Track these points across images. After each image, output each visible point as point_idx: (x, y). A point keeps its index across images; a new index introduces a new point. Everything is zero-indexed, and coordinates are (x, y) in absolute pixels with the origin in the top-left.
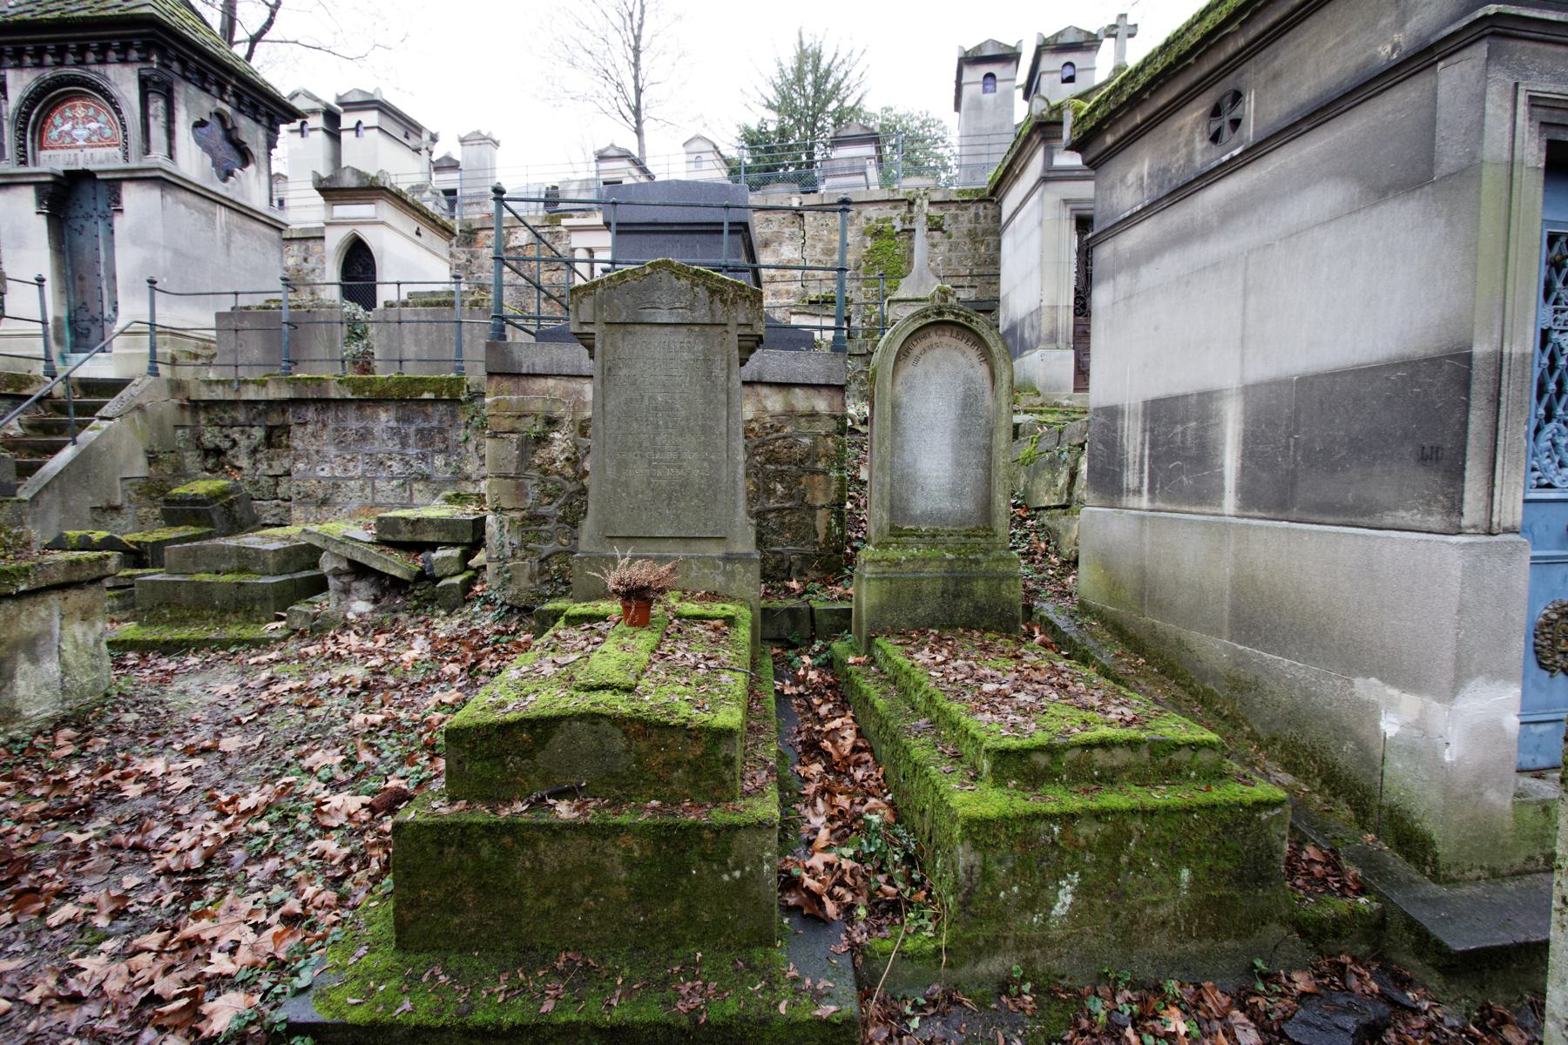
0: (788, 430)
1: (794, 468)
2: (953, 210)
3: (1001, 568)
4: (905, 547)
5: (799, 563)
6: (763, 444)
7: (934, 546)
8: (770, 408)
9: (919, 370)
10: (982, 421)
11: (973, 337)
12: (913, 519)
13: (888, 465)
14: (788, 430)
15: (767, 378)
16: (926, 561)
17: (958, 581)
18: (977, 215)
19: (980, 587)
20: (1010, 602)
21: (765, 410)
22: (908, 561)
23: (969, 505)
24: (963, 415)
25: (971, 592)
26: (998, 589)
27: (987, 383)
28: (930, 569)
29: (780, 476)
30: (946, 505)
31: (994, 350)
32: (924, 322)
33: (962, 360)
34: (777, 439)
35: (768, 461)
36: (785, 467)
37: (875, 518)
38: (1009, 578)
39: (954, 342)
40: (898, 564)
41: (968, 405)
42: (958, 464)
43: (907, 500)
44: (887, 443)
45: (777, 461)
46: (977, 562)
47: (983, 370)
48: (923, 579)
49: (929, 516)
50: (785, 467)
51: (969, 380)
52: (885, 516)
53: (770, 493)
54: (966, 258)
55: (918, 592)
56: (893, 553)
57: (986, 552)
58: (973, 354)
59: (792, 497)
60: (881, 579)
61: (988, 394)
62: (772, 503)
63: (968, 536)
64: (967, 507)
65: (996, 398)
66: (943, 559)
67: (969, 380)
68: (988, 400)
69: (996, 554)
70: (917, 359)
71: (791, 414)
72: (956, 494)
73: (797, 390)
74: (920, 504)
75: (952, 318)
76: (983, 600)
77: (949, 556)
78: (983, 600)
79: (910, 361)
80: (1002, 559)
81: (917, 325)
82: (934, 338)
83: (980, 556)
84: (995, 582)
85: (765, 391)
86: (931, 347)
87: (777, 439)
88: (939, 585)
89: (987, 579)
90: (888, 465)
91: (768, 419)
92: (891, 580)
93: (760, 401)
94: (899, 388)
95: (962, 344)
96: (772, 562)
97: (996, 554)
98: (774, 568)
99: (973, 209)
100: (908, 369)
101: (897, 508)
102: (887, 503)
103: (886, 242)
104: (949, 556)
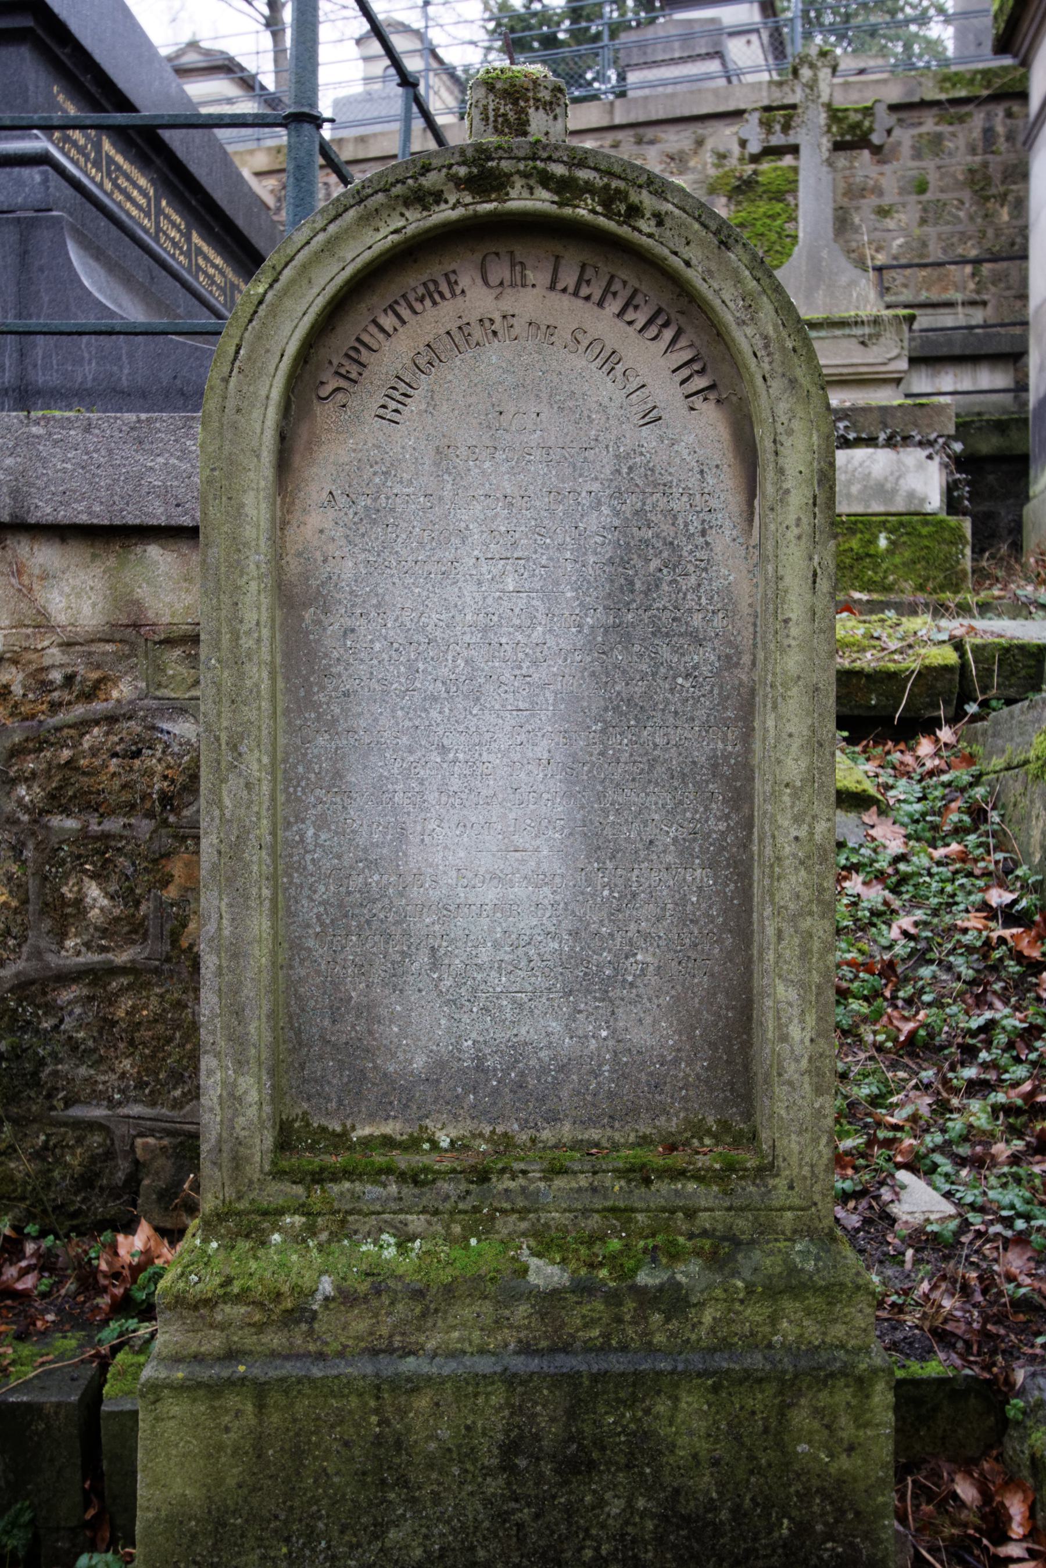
0: (123, 691)
1: (145, 826)
2: (929, 124)
3: (794, 1325)
4: (342, 1230)
5: (164, 1165)
6: (39, 743)
7: (480, 1223)
8: (61, 618)
9: (408, 438)
10: (706, 657)
11: (654, 296)
12: (398, 1094)
13: (258, 861)
14: (123, 691)
15: (44, 511)
16: (429, 1299)
17: (580, 1394)
18: (989, 133)
19: (687, 1422)
20: (837, 1493)
21: (43, 623)
22: (346, 1298)
23: (649, 1028)
24: (619, 632)
25: (643, 1447)
26: (777, 1434)
27: (724, 487)
28: (459, 1338)
29: (99, 854)
30: (547, 1030)
31: (744, 338)
32: (416, 221)
33: (604, 390)
34: (84, 725)
35: (56, 802)
36: (113, 825)
37: (233, 1097)
38: (825, 1377)
39: (567, 312)
40: (299, 1314)
41: (639, 590)
42: (596, 845)
43: (368, 1011)
44: (255, 762)
45: (90, 803)
46: (674, 1301)
47: (704, 431)
48: (414, 1385)
49: (465, 1081)
50: (113, 825)
51: (639, 483)
52: (252, 1089)
53: (65, 915)
54: (964, 238)
55: (390, 1446)
56: (290, 1260)
57: (722, 1251)
58: (654, 363)
59: (135, 930)
60: (215, 1390)
61: (725, 539)
62: (73, 952)
63: (641, 1175)
64: (640, 1037)
65: (761, 555)
66: (510, 1287)
67: (639, 483)
68: (729, 564)
69: (765, 1261)
70: (400, 392)
71: (132, 634)
72: (589, 979)
73: (154, 551)
74: (424, 1029)
75: (543, 201)
76: (706, 1481)
77: (545, 1273)
78: (706, 1481)
79: (368, 399)
80: (791, 1285)
81: (380, 238)
82: (476, 299)
83: (688, 1272)
84: (760, 1400)
85: (44, 556)
86: (462, 336)
87: (84, 725)
88: (492, 1412)
89: (719, 1384)
90: (258, 861)
91: (55, 655)
92: (260, 1391)
93: (26, 593)
94: (317, 522)
95: (604, 323)
96: (74, 1160)
97: (765, 1261)
98: (87, 1181)
99: (978, 119)
100: (350, 442)
101: (318, 1047)
102: (257, 1029)
103: (763, 207)
104: (545, 1273)
